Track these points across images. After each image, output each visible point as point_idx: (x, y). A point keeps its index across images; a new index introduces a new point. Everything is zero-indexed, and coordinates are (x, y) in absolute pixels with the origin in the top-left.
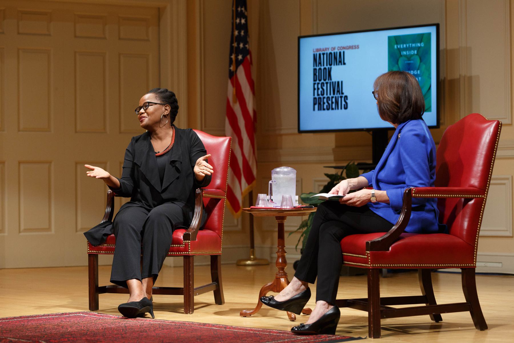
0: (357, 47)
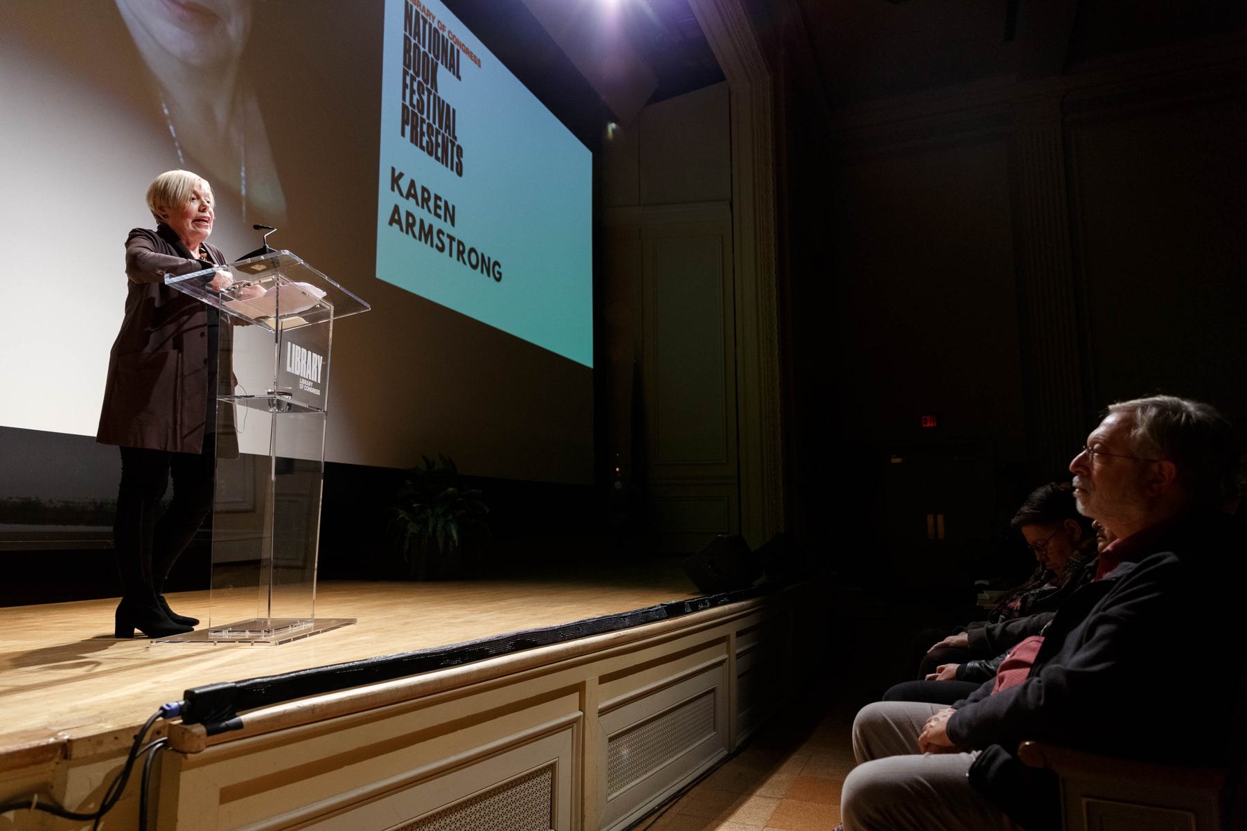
0: (478, 62)
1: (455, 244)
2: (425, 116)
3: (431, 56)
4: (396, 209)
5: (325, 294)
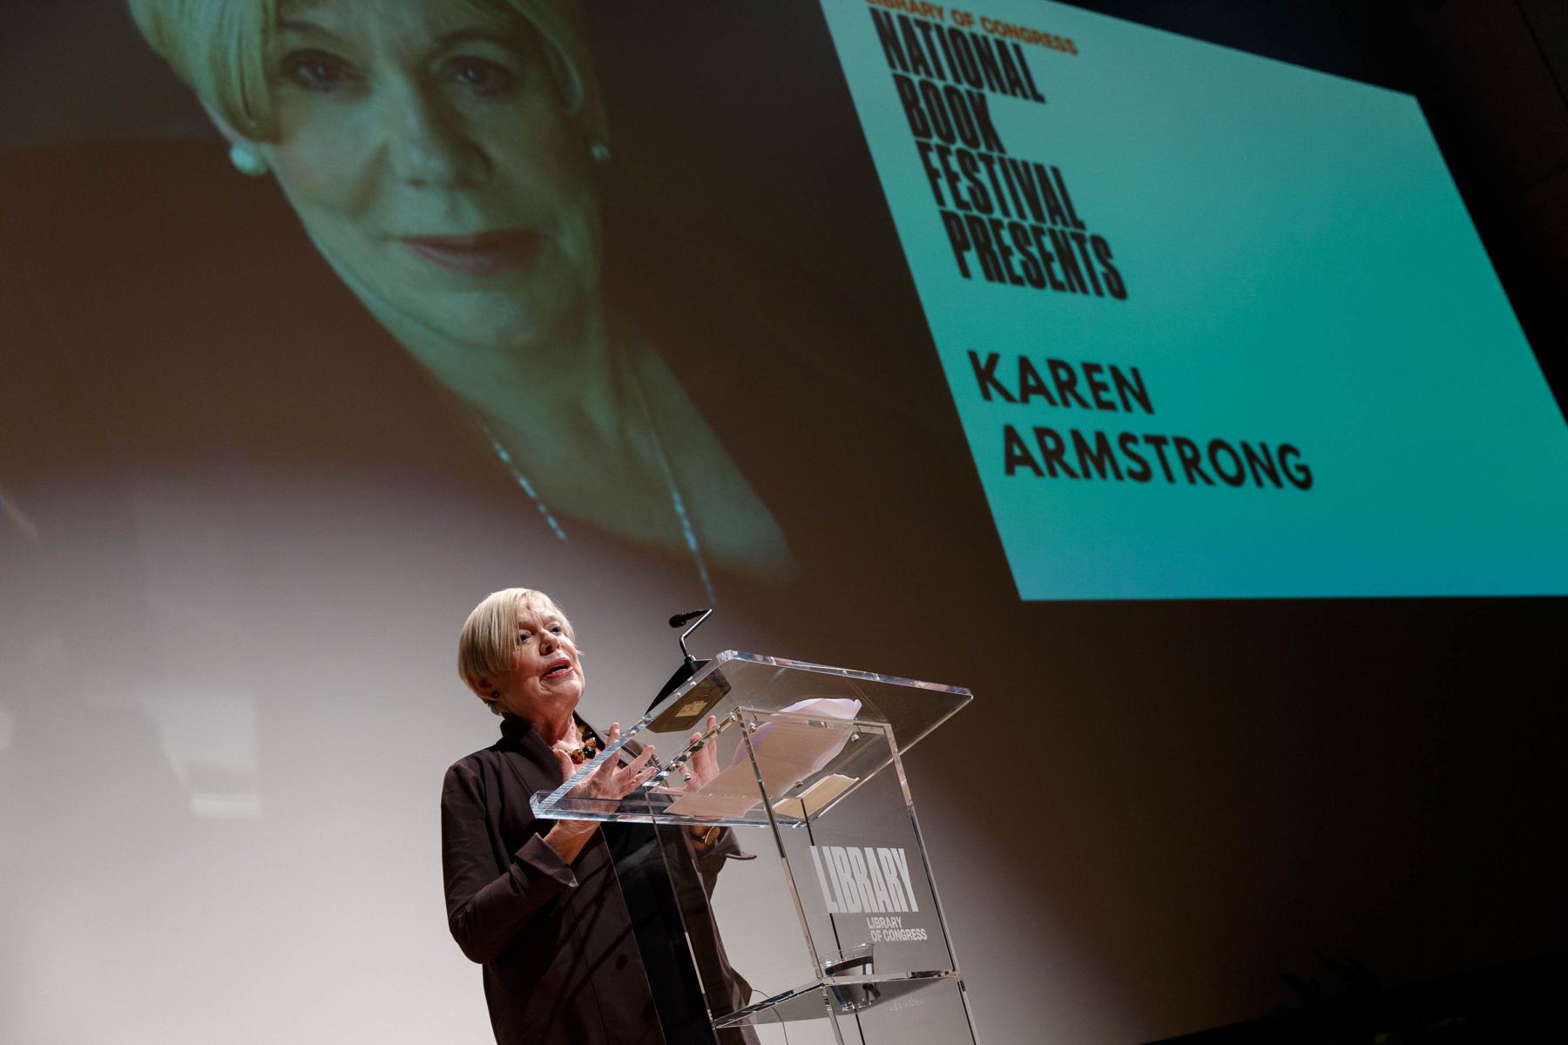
0: (1067, 46)
1: (1170, 451)
2: (997, 214)
3: (964, 87)
4: (1011, 435)
5: (857, 704)
